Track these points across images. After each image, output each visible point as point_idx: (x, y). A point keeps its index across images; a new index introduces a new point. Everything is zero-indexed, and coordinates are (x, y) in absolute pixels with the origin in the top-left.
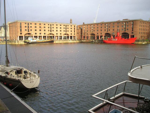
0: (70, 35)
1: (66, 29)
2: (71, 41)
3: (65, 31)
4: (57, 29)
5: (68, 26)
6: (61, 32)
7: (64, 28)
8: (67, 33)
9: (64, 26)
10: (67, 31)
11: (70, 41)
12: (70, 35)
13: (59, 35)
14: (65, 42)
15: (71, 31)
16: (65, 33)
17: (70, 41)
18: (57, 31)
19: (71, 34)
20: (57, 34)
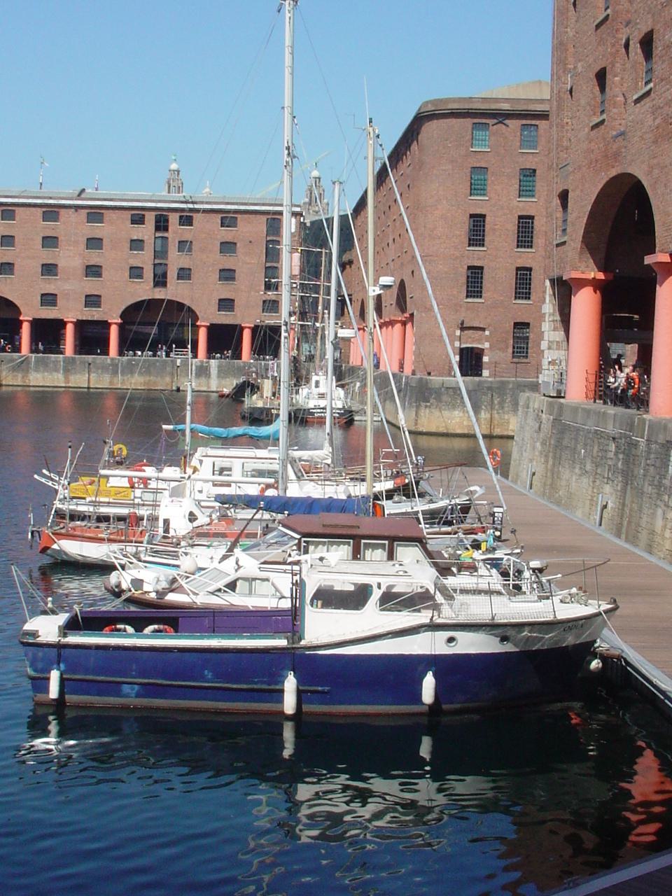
0: (208, 315)
1: (161, 253)
2: (222, 373)
3: (149, 274)
4: (47, 256)
5: (186, 220)
6: (92, 286)
7: (137, 244)
8: (175, 291)
9: (138, 220)
10: (172, 274)
11: (203, 371)
12: (208, 315)
13: (71, 312)
14: (136, 382)
15: (227, 275)
16: (145, 290)
17: (203, 371)
18: (49, 269)
19: (226, 304)
20: (49, 299)
